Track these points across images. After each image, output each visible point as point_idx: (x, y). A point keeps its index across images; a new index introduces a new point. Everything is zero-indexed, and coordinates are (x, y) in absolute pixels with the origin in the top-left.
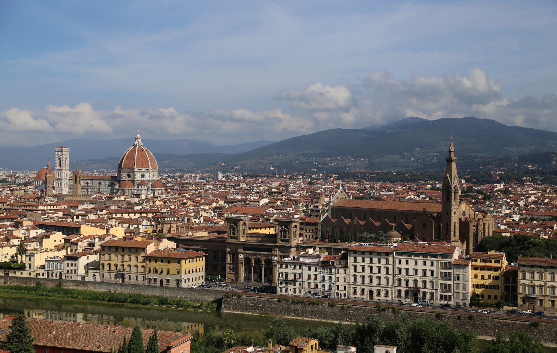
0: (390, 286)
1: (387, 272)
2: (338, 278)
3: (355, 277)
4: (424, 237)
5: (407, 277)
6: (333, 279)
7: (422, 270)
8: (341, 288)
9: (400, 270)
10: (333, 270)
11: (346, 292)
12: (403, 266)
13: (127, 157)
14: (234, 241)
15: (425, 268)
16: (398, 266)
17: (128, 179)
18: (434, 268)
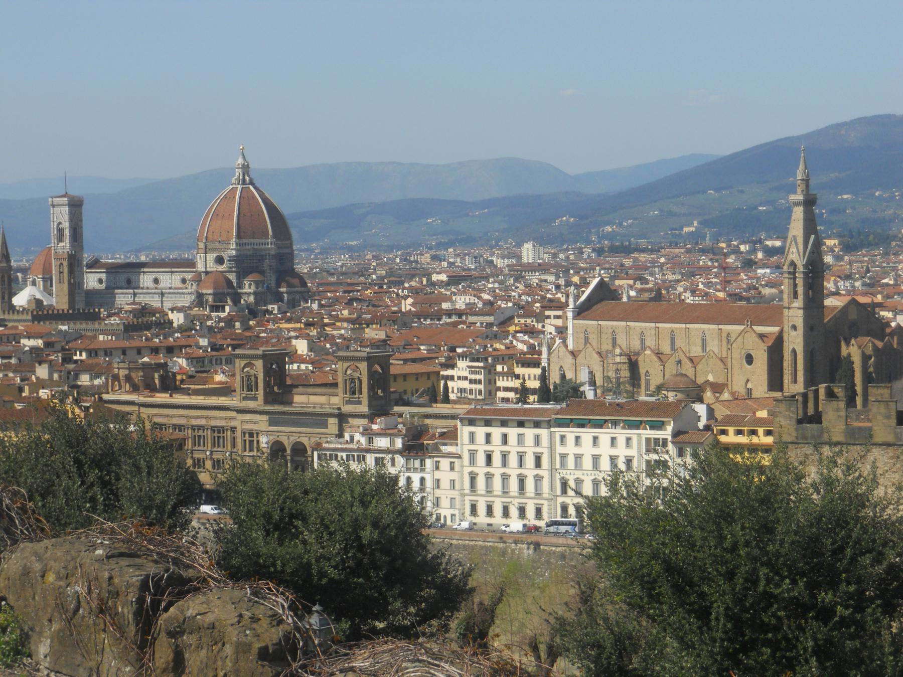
0: (545, 496)
1: (538, 464)
2: (438, 480)
3: (473, 478)
4: (749, 386)
5: (578, 474)
6: (429, 484)
7: (611, 456)
8: (445, 502)
9: (563, 457)
10: (429, 463)
11: (456, 512)
12: (570, 449)
13: (216, 215)
14: (251, 404)
15: (614, 452)
16: (560, 449)
17: (221, 268)
18: (633, 452)
